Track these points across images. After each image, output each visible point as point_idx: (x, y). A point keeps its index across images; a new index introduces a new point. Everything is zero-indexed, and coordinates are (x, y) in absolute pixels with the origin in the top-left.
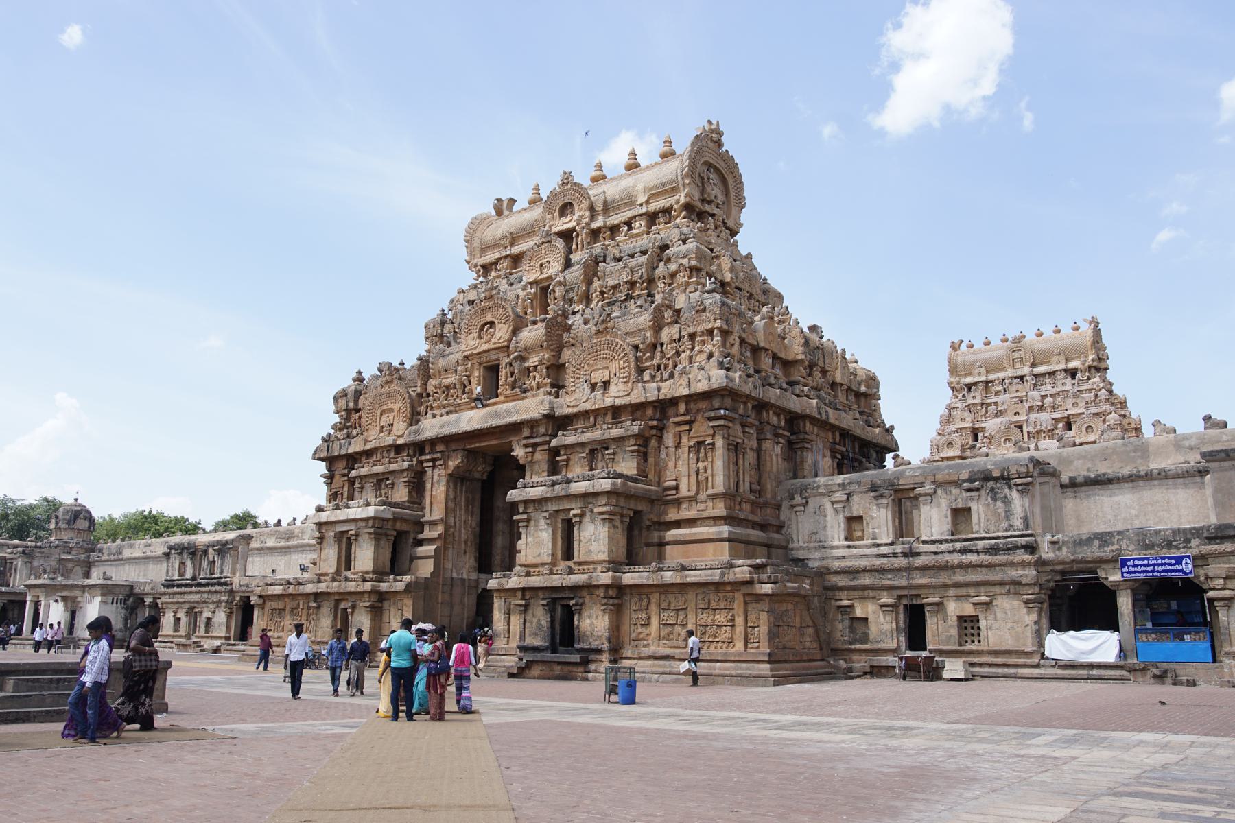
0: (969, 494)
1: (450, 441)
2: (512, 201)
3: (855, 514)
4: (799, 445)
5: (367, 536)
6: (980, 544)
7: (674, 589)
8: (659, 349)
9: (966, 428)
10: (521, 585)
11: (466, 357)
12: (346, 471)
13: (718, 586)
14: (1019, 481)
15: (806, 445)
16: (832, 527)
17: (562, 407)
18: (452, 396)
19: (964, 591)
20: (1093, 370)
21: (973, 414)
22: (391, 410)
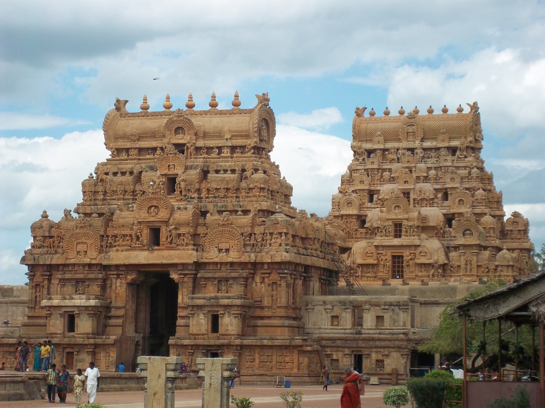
0: (384, 311)
3: (335, 315)
6: (387, 331)
9: (364, 190)
10: (192, 344)
11: (139, 222)
12: (48, 273)
13: (286, 347)
14: (403, 307)
15: (312, 279)
16: (325, 320)
17: (202, 258)
18: (128, 241)
19: (379, 350)
20: (469, 150)
21: (370, 177)
22: (86, 243)
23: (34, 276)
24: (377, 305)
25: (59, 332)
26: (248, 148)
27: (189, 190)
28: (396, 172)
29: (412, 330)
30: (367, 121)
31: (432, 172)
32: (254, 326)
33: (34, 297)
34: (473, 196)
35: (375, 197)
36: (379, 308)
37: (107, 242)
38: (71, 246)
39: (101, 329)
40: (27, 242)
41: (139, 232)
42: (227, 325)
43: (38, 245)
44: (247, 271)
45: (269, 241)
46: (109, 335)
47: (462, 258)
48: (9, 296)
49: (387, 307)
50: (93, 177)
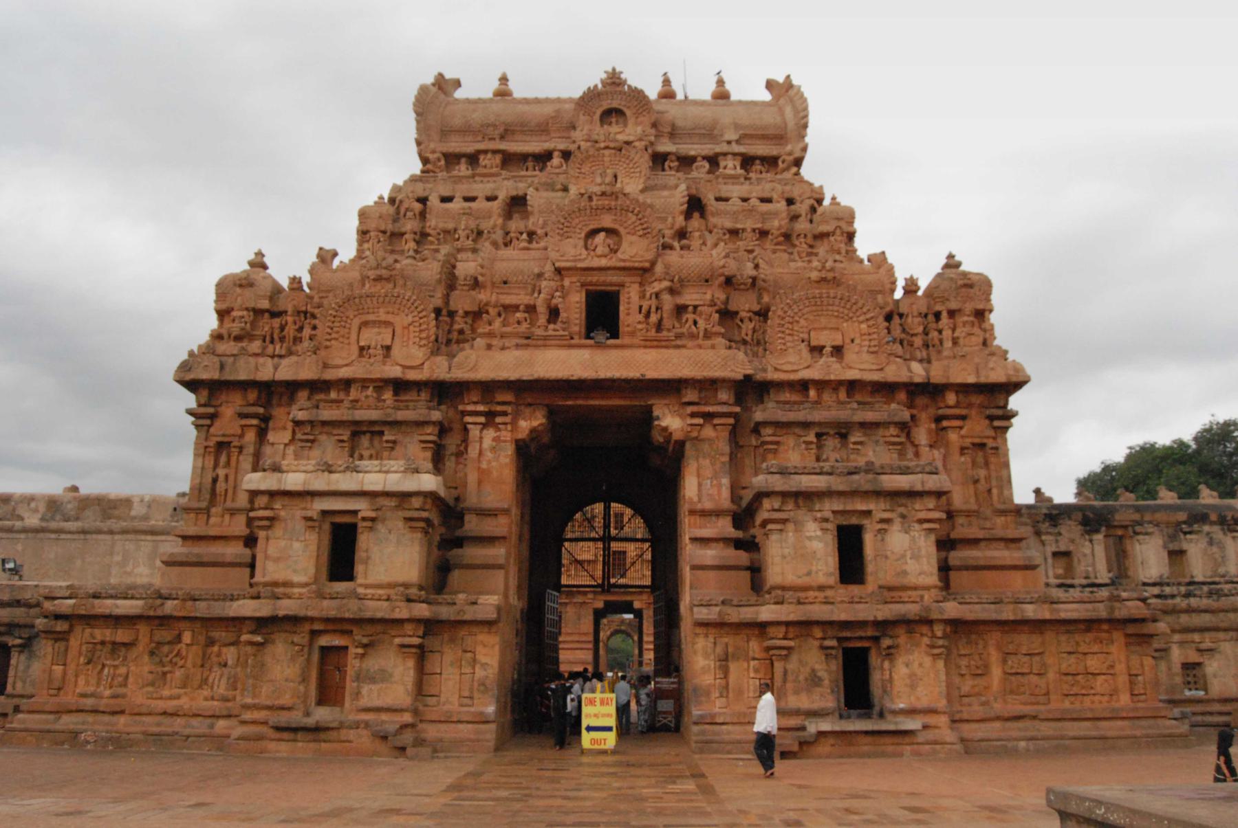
3: (1063, 548)
5: (401, 524)
8: (896, 317)
10: (792, 617)
11: (559, 271)
12: (261, 410)
13: (1090, 624)
17: (765, 370)
18: (519, 323)
19: (1189, 637)
22: (387, 324)
23: (213, 417)
25: (296, 579)
37: (449, 332)
38: (347, 330)
42: (903, 556)
43: (236, 332)
45: (950, 332)
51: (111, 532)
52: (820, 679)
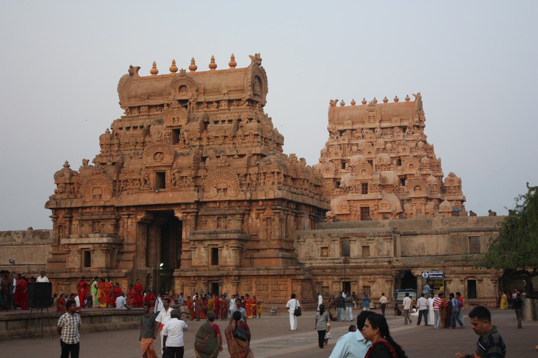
0: (369, 241)
1: (139, 207)
2: (139, 68)
3: (324, 246)
4: (300, 215)
5: (100, 251)
6: (372, 260)
7: (263, 277)
8: (248, 175)
10: (194, 275)
11: (147, 167)
12: (69, 216)
13: (281, 276)
15: (302, 215)
16: (315, 251)
17: (203, 198)
18: (137, 184)
19: (365, 277)
20: (416, 128)
21: (342, 150)
23: (57, 218)
24: (363, 236)
25: (77, 267)
26: (243, 101)
27: (191, 139)
28: (361, 145)
29: (396, 258)
30: (339, 109)
31: (389, 145)
32: (251, 258)
33: (57, 237)
34: (420, 161)
35: (347, 164)
36: (365, 239)
37: (120, 187)
38: (88, 191)
39: (114, 264)
40: (51, 188)
41: (147, 176)
43: (61, 191)
44: (244, 208)
46: (122, 269)
47: (414, 208)
48: (46, 239)
49: (372, 238)
50: (109, 132)
51: (44, 244)
52: (204, 292)
